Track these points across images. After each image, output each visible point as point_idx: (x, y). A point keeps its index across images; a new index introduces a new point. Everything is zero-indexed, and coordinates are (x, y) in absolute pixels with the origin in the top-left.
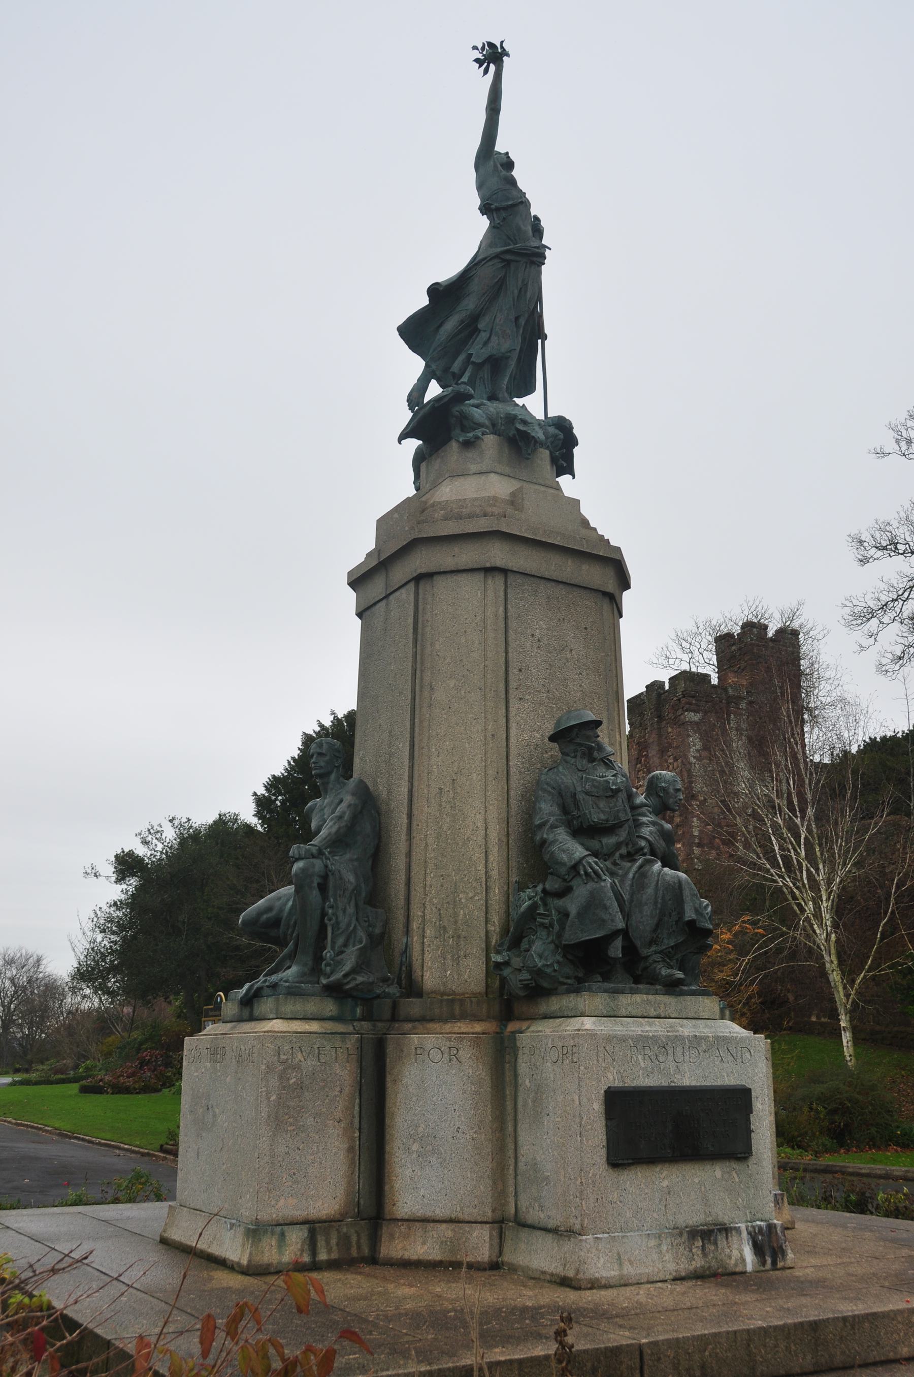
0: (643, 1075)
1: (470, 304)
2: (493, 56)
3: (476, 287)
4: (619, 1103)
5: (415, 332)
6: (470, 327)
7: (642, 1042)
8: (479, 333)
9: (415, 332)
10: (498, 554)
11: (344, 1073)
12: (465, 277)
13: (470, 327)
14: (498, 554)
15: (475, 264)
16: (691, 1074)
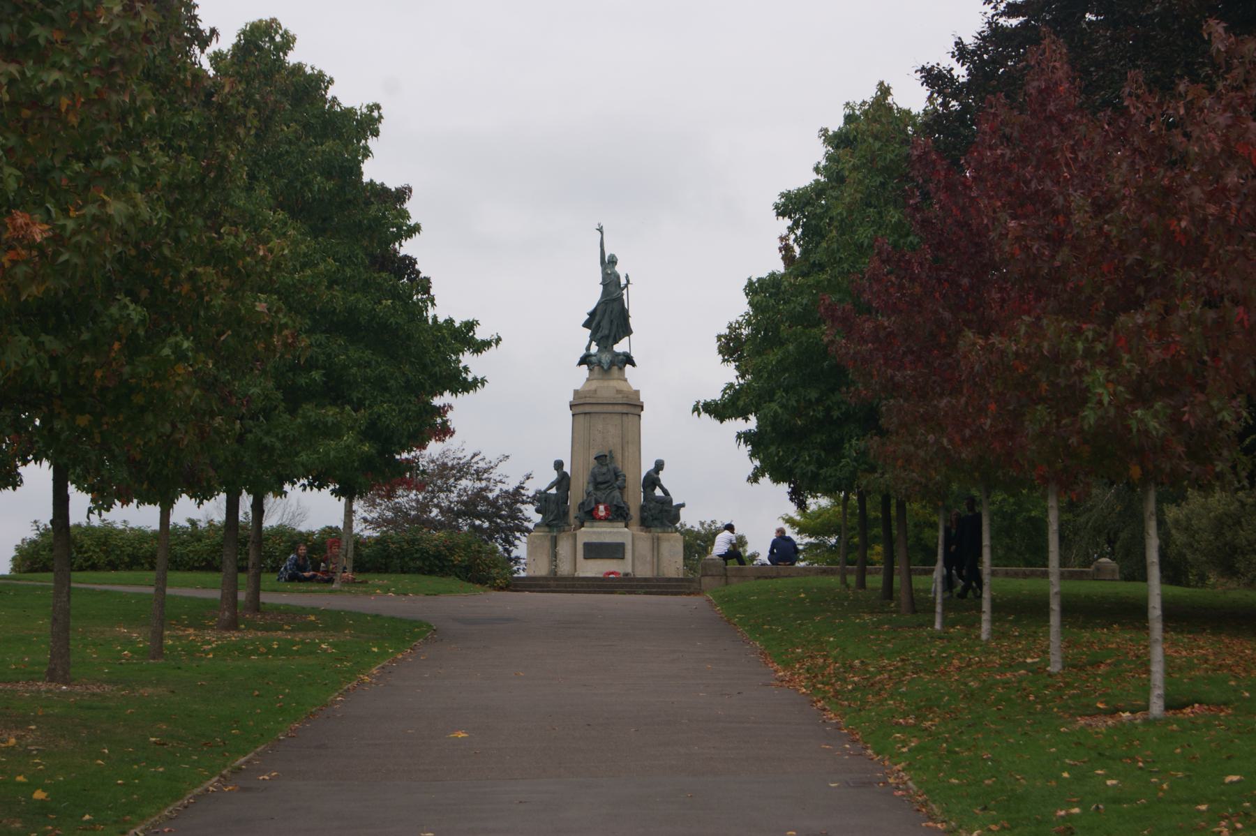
0: (594, 539)
1: (597, 318)
2: (601, 230)
3: (598, 312)
4: (585, 544)
5: (587, 325)
6: (599, 325)
7: (594, 533)
8: (610, 320)
9: (587, 325)
10: (587, 409)
11: (547, 544)
12: (595, 309)
13: (599, 325)
14: (587, 409)
15: (599, 304)
16: (608, 540)
